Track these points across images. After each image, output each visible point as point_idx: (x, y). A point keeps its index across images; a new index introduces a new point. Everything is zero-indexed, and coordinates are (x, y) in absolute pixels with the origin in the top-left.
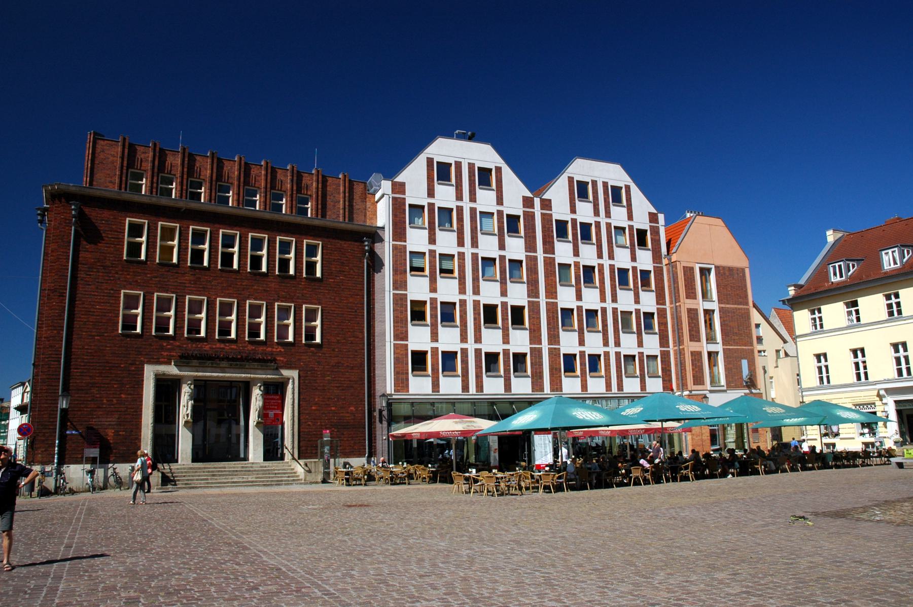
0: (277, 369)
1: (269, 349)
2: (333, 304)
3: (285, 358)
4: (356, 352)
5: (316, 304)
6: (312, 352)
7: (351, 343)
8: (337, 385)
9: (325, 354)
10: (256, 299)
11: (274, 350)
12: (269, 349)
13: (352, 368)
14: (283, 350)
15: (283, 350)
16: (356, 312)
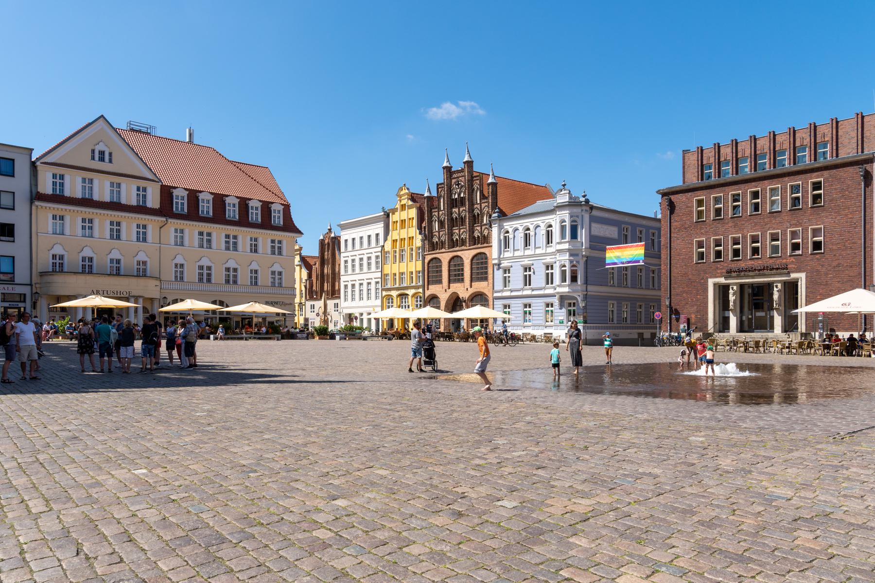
0: (789, 273)
1: (785, 261)
2: (834, 222)
3: (796, 265)
4: (855, 254)
5: (820, 225)
6: (817, 259)
7: (851, 248)
8: (838, 280)
9: (827, 259)
10: (774, 229)
11: (788, 261)
12: (785, 261)
13: (851, 267)
14: (794, 260)
15: (794, 260)
16: (855, 224)
